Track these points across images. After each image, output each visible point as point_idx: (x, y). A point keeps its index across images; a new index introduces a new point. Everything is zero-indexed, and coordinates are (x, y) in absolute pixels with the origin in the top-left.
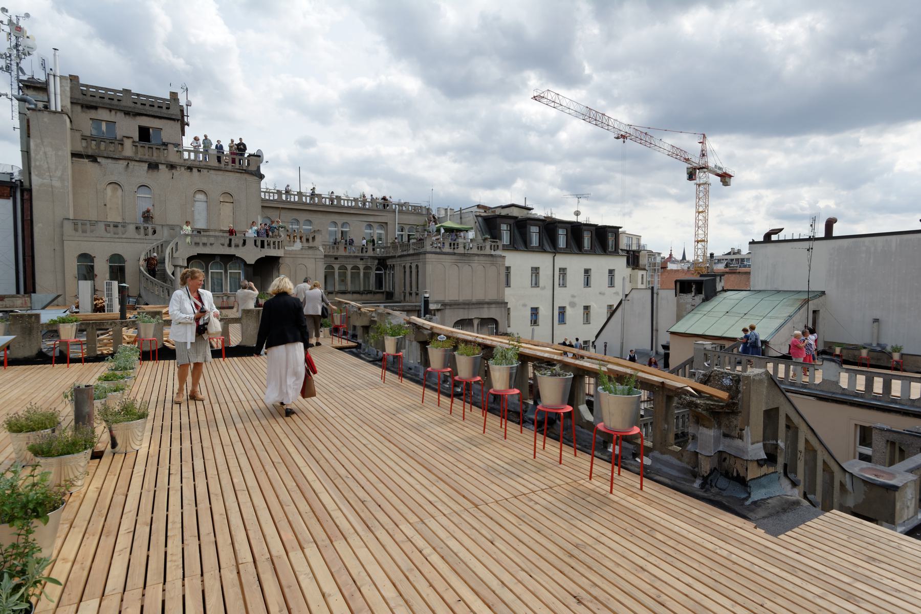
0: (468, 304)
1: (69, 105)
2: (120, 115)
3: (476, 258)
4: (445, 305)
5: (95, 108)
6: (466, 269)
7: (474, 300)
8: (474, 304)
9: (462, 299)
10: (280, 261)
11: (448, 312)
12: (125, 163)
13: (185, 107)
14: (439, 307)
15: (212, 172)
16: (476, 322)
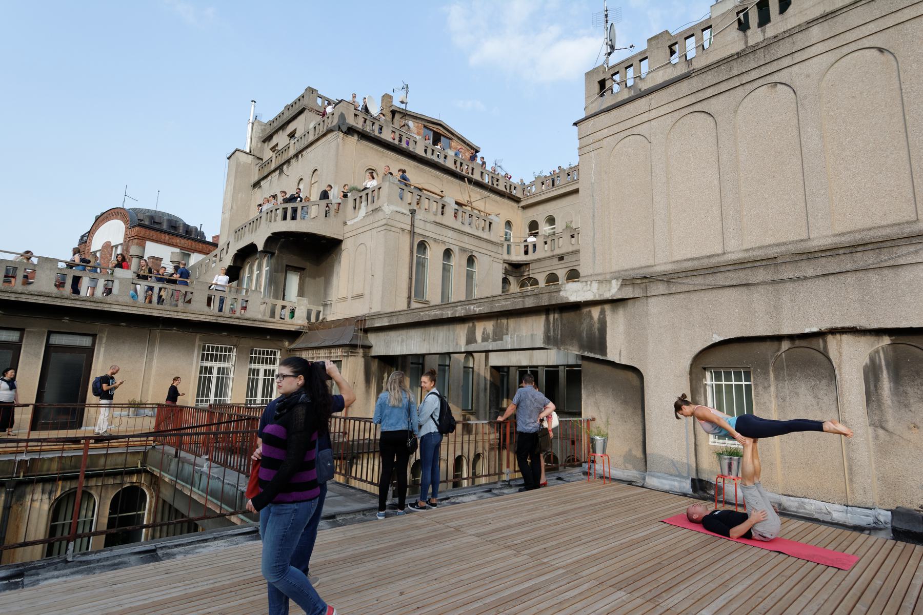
0: (770, 262)
1: (257, 144)
2: (281, 132)
3: (816, 32)
4: (642, 280)
5: (269, 138)
6: (759, 111)
7: (821, 237)
8: (809, 256)
9: (735, 249)
10: (343, 246)
11: (657, 308)
12: (269, 178)
13: (403, 106)
14: (613, 291)
15: (309, 150)
16: (851, 357)
